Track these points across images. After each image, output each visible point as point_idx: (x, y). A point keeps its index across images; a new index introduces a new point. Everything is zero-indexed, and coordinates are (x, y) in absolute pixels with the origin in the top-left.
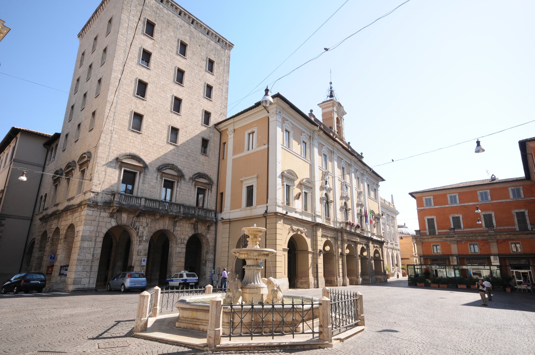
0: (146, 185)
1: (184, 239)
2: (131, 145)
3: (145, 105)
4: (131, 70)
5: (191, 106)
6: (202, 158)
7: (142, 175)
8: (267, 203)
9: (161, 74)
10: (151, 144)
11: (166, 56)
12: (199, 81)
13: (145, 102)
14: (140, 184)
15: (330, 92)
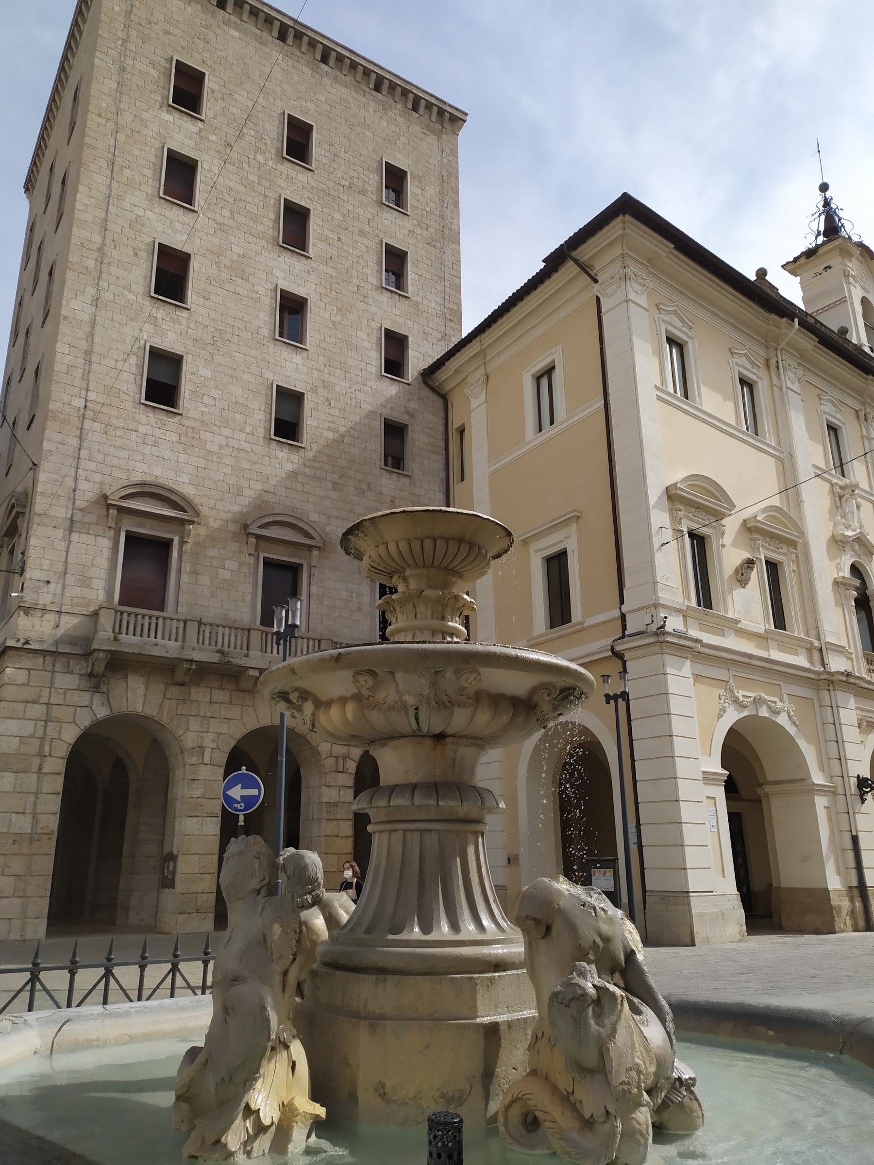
0: (205, 580)
1: (346, 757)
2: (147, 452)
3: (184, 322)
4: (133, 217)
5: (338, 319)
8: (622, 602)
9: (231, 222)
10: (215, 448)
11: (245, 166)
12: (359, 238)
13: (185, 314)
14: (185, 578)
15: (823, 217)
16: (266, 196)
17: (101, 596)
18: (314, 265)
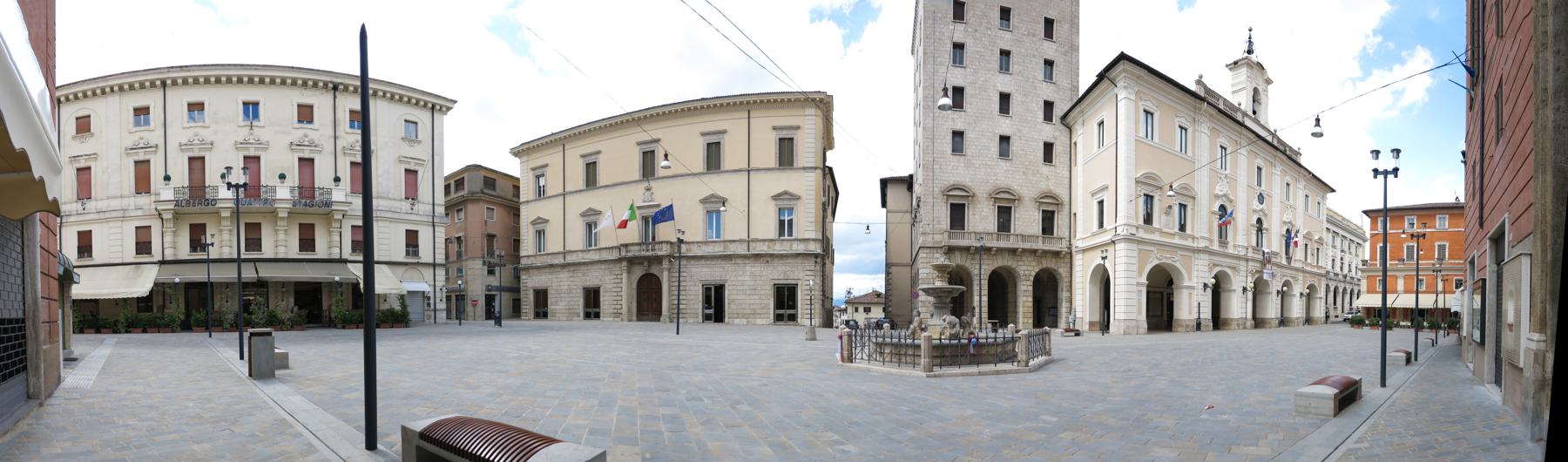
0: (977, 216)
5: (1023, 100)
6: (1046, 169)
7: (970, 206)
12: (1033, 59)
13: (963, 113)
14: (970, 217)
16: (992, 50)
17: (945, 227)
18: (1013, 76)
